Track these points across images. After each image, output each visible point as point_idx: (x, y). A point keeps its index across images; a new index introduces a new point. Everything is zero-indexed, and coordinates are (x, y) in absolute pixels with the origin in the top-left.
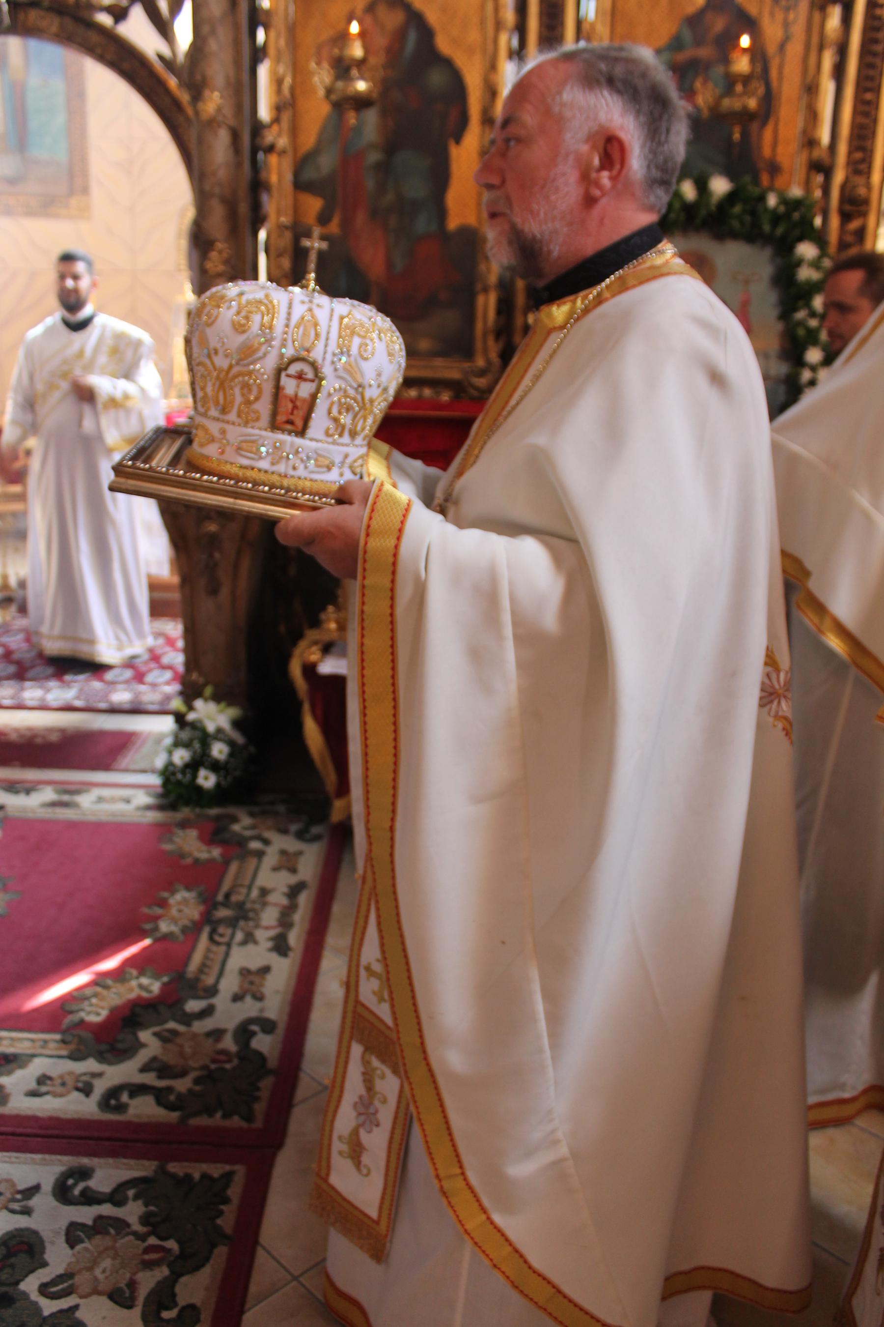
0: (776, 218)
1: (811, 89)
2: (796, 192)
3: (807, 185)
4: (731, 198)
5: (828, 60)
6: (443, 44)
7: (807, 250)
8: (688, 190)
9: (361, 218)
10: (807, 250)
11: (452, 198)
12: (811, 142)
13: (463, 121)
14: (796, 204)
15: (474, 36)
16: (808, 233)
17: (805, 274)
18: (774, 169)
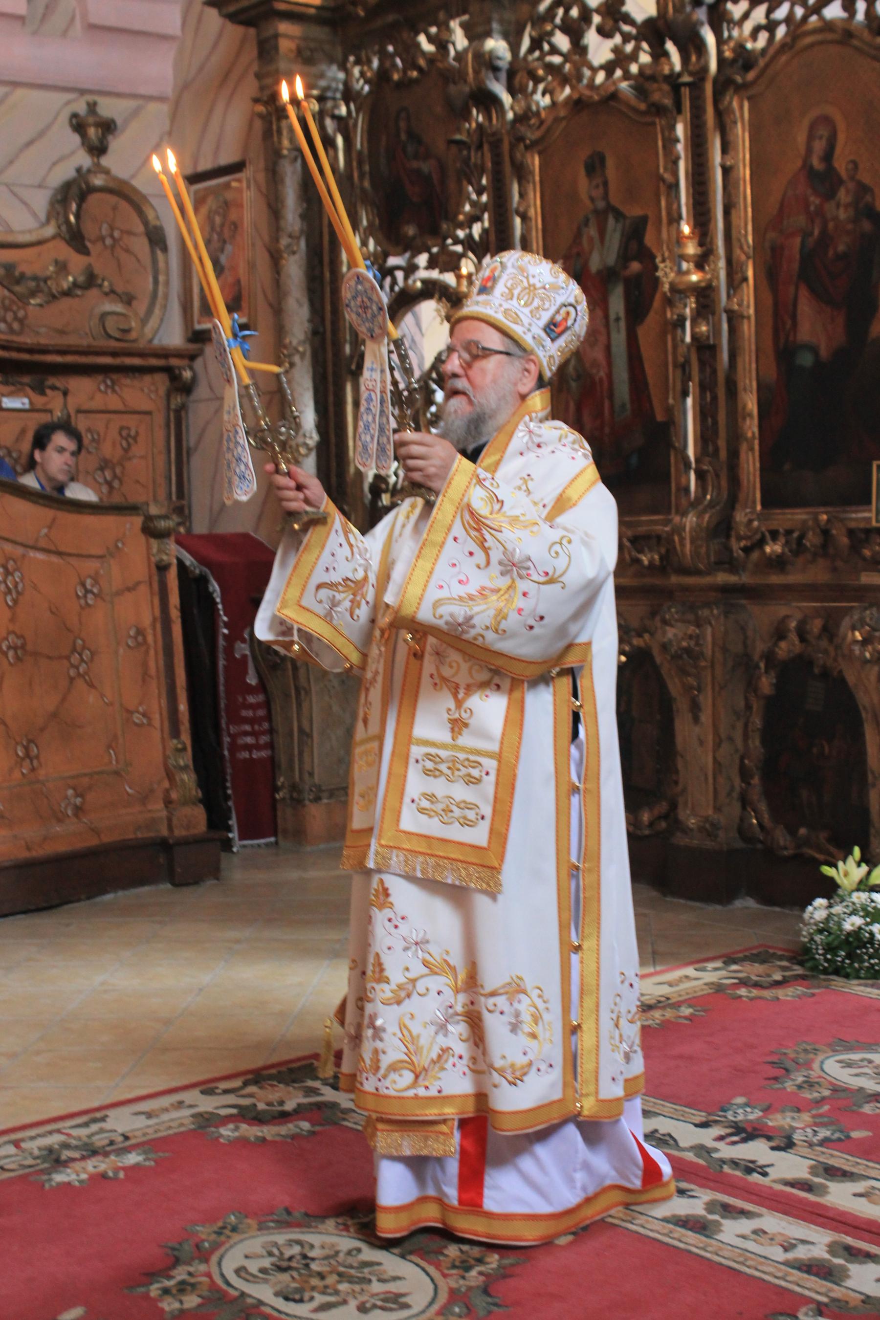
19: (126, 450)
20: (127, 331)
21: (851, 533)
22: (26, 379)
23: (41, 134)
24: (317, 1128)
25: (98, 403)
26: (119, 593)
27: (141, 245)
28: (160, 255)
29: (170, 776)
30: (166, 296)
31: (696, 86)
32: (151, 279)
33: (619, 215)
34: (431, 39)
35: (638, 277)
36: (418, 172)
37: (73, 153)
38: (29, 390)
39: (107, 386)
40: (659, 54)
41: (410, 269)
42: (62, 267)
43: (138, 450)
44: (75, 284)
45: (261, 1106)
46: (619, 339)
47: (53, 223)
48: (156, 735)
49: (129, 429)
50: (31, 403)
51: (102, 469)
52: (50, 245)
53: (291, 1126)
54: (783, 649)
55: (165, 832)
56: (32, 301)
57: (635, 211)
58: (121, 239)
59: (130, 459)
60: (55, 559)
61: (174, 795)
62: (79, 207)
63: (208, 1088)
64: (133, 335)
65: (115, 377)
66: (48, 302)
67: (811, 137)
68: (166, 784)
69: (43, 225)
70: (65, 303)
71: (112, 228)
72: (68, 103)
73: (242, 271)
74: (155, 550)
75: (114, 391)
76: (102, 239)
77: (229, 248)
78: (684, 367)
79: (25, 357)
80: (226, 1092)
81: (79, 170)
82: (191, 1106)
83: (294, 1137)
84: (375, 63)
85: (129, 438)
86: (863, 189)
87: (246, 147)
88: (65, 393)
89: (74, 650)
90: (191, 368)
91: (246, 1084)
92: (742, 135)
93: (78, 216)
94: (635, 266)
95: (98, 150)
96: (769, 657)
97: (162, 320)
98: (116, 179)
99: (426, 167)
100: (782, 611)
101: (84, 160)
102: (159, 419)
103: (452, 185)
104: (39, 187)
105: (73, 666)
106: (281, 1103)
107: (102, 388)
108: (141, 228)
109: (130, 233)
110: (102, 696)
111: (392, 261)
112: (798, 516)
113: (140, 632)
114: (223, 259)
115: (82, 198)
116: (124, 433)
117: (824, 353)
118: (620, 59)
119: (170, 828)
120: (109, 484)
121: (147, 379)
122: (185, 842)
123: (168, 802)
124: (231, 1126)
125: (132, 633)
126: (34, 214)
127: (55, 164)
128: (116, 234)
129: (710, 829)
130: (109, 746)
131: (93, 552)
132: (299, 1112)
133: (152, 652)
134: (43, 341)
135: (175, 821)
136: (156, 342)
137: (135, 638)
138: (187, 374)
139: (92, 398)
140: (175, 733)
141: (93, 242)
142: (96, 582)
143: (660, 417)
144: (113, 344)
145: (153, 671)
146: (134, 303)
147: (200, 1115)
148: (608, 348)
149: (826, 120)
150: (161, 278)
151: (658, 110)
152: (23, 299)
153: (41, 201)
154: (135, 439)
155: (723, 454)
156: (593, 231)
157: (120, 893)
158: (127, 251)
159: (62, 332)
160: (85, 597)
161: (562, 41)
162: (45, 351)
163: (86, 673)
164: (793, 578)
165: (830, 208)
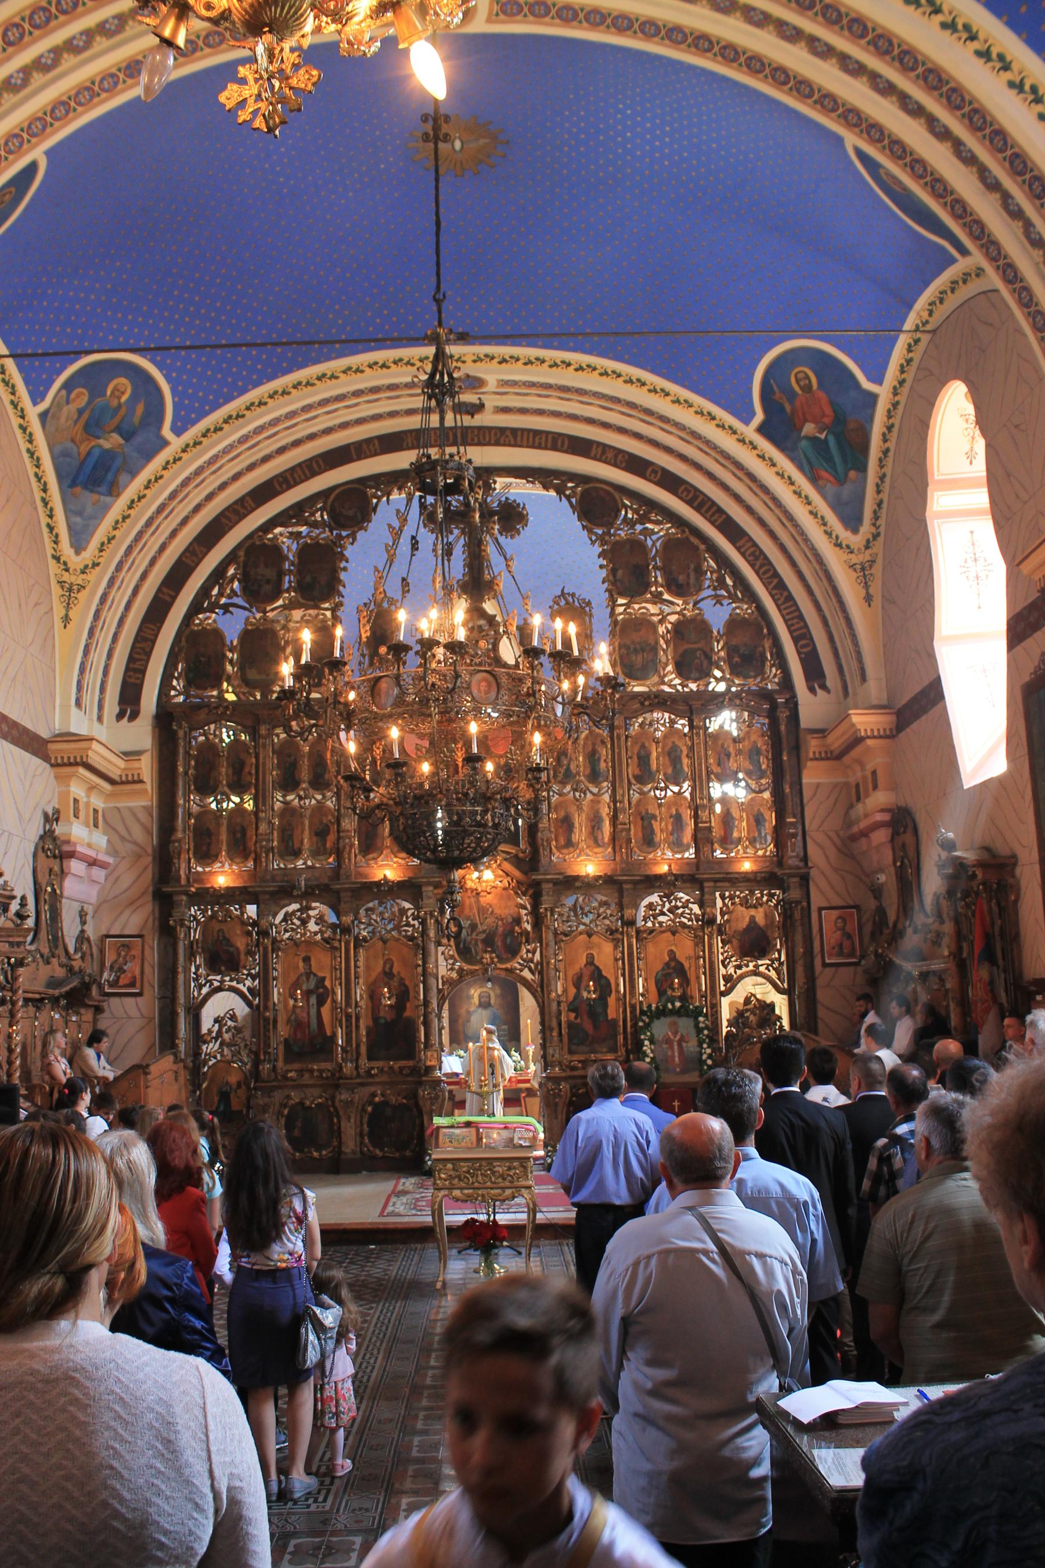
0: (693, 1011)
1: (698, 978)
2: (697, 1004)
3: (700, 1001)
4: (681, 1007)
5: (702, 970)
6: (604, 973)
7: (701, 1019)
8: (670, 1006)
9: (585, 1017)
10: (701, 1019)
11: (609, 1011)
12: (700, 990)
13: (611, 992)
14: (697, 1007)
15: (612, 971)
16: (700, 1013)
17: (701, 1025)
18: (692, 997)
21: (400, 1068)
31: (347, 944)
33: (315, 975)
34: (236, 910)
35: (322, 994)
36: (228, 951)
40: (334, 933)
41: (222, 982)
46: (313, 1011)
54: (377, 1099)
57: (320, 974)
67: (385, 963)
73: (137, 972)
77: (129, 964)
78: (341, 1021)
84: (210, 913)
86: (402, 979)
87: (142, 929)
92: (362, 958)
94: (321, 990)
96: (371, 1103)
99: (231, 949)
100: (373, 1089)
103: (242, 957)
111: (210, 978)
112: (380, 1064)
114: (125, 968)
117: (388, 1019)
118: (321, 931)
129: (354, 1152)
143: (329, 1033)
148: (308, 1013)
149: (390, 959)
151: (336, 948)
155: (354, 1046)
156: (304, 978)
161: (297, 922)
164: (377, 1080)
165: (392, 982)
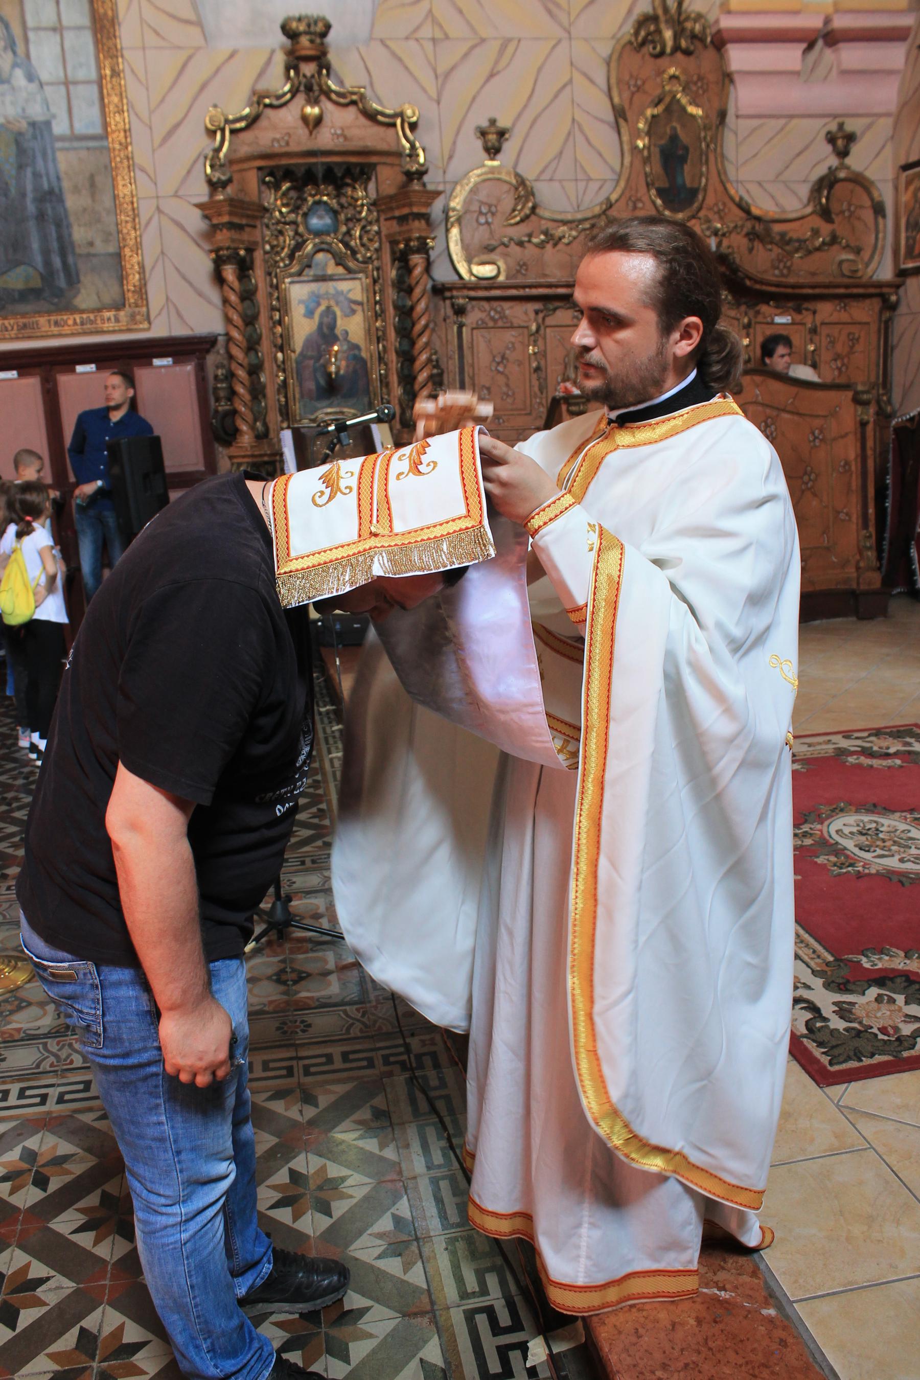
19: (852, 347)
20: (856, 271)
22: (790, 304)
23: (806, 148)
24: (904, 764)
25: (835, 318)
26: (835, 439)
27: (868, 215)
28: (880, 220)
29: (860, 552)
30: (883, 247)
32: (873, 236)
37: (827, 157)
38: (791, 311)
39: (841, 308)
42: (816, 232)
43: (859, 348)
44: (824, 243)
45: (875, 748)
47: (812, 204)
48: (854, 527)
49: (854, 334)
50: (792, 319)
51: (835, 360)
52: (810, 218)
53: (889, 761)
55: (854, 586)
56: (796, 255)
58: (854, 212)
59: (854, 353)
60: (796, 418)
61: (862, 564)
62: (829, 193)
63: (847, 735)
64: (860, 274)
65: (846, 301)
66: (806, 255)
68: (858, 557)
69: (805, 207)
70: (817, 255)
71: (850, 205)
72: (825, 125)
74: (859, 412)
75: (845, 310)
76: (842, 212)
79: (789, 291)
80: (857, 738)
81: (830, 168)
82: (834, 744)
83: (889, 767)
85: (853, 340)
88: (814, 312)
89: (805, 473)
90: (897, 294)
91: (869, 735)
93: (827, 198)
95: (843, 154)
97: (879, 263)
98: (854, 173)
101: (834, 161)
102: (874, 327)
104: (804, 181)
105: (803, 483)
106: (888, 748)
107: (838, 308)
108: (868, 203)
109: (861, 207)
110: (821, 501)
113: (847, 463)
115: (831, 186)
116: (851, 337)
119: (858, 584)
120: (839, 369)
121: (868, 301)
122: (866, 593)
123: (858, 568)
124: (855, 757)
125: (842, 463)
126: (800, 199)
127: (815, 166)
128: (852, 208)
130: (824, 533)
131: (821, 413)
132: (896, 755)
133: (854, 476)
134: (801, 281)
135: (861, 580)
136: (875, 278)
137: (844, 466)
138: (893, 298)
139: (831, 315)
140: (865, 526)
141: (837, 215)
142: (821, 432)
144: (846, 281)
145: (854, 487)
146: (862, 253)
147: (839, 749)
150: (881, 235)
152: (790, 254)
153: (804, 191)
154: (858, 340)
157: (824, 621)
158: (859, 218)
159: (813, 274)
160: (814, 440)
162: (802, 286)
163: (812, 487)
